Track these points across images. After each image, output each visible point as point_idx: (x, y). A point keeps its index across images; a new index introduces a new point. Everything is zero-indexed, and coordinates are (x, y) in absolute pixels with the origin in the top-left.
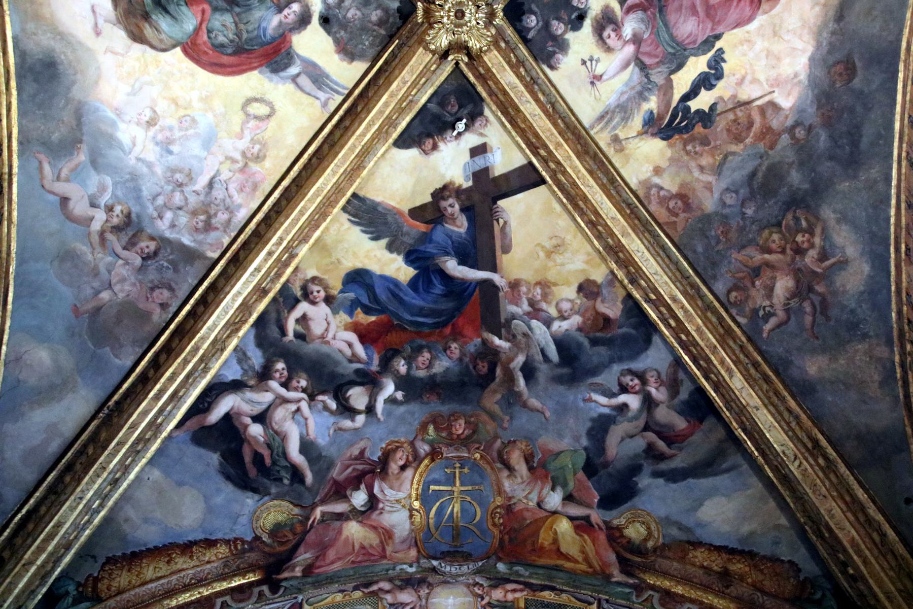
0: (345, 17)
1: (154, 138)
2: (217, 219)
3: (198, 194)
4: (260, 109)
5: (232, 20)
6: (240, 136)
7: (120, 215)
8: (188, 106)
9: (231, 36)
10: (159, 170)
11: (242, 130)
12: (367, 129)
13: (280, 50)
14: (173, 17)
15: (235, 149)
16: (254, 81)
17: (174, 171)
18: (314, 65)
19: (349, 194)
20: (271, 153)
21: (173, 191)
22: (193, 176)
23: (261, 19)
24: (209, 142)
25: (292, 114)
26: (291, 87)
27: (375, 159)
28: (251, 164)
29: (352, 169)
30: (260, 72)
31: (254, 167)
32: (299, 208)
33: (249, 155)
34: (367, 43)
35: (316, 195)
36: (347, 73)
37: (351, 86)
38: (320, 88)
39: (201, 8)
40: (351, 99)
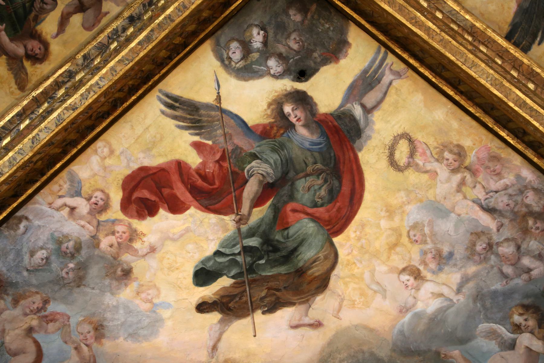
0: (298, 52)
1: (434, 272)
2: (534, 204)
3: (502, 225)
4: (402, 152)
5: (303, 180)
6: (434, 174)
7: (525, 317)
8: (396, 231)
9: (320, 182)
10: (472, 269)
11: (426, 172)
12: (421, 26)
13: (335, 126)
14: (301, 243)
15: (448, 180)
16: (371, 157)
17: (471, 253)
18: (352, 88)
19: (504, 43)
20: (455, 139)
21: (497, 255)
22: (480, 230)
23: (303, 149)
24: (438, 210)
25: (408, 112)
26: (376, 116)
27: (462, 13)
28: (467, 162)
29: (471, 43)
30: (360, 150)
31: (471, 158)
32: (516, 108)
33: (457, 164)
34: (327, 26)
35: (500, 87)
36: (361, 50)
37: (376, 44)
38: (379, 81)
39: (291, 214)
40: (390, 44)
